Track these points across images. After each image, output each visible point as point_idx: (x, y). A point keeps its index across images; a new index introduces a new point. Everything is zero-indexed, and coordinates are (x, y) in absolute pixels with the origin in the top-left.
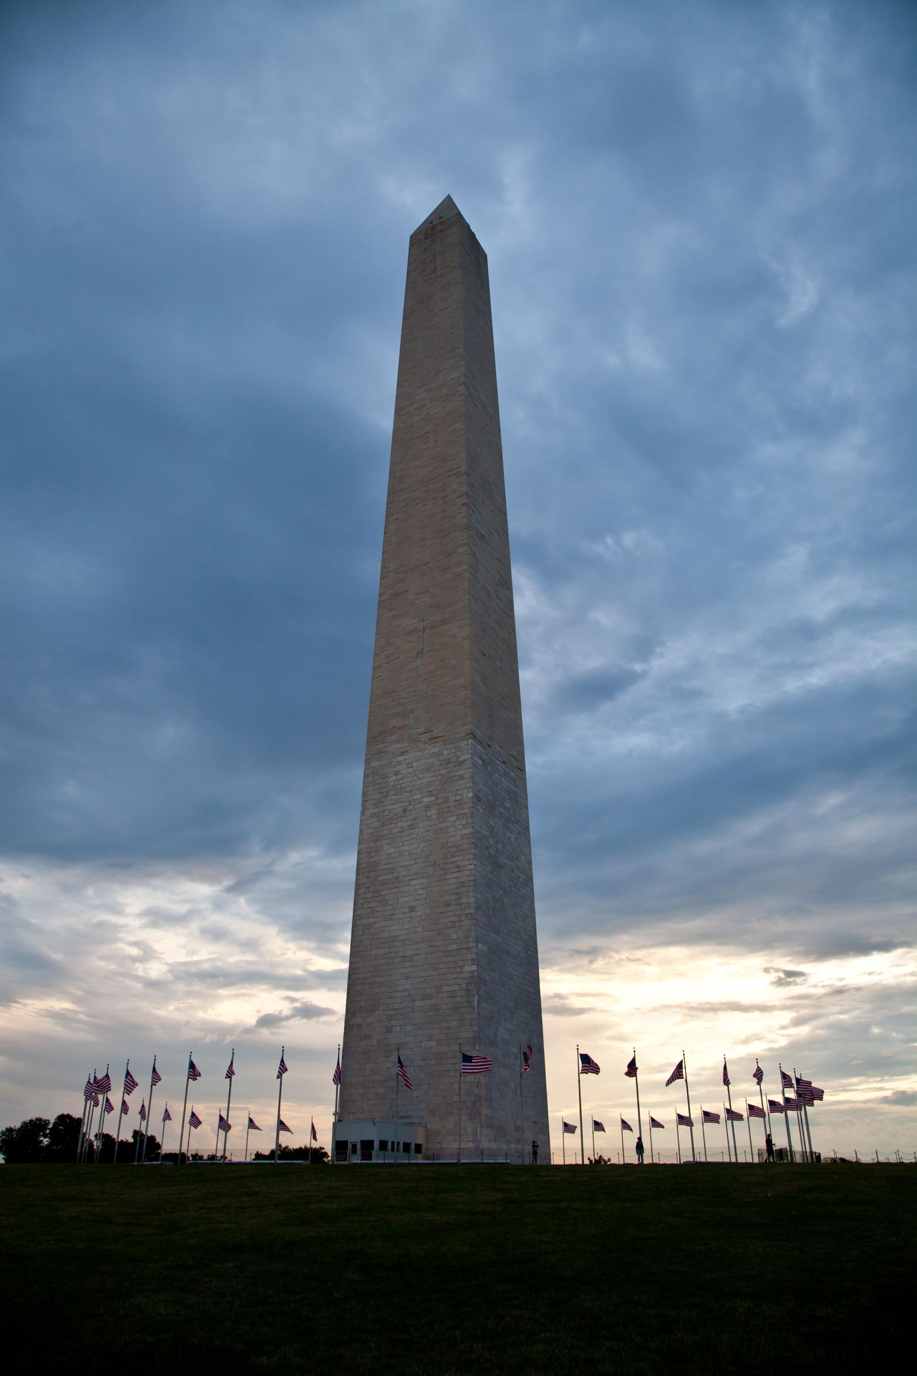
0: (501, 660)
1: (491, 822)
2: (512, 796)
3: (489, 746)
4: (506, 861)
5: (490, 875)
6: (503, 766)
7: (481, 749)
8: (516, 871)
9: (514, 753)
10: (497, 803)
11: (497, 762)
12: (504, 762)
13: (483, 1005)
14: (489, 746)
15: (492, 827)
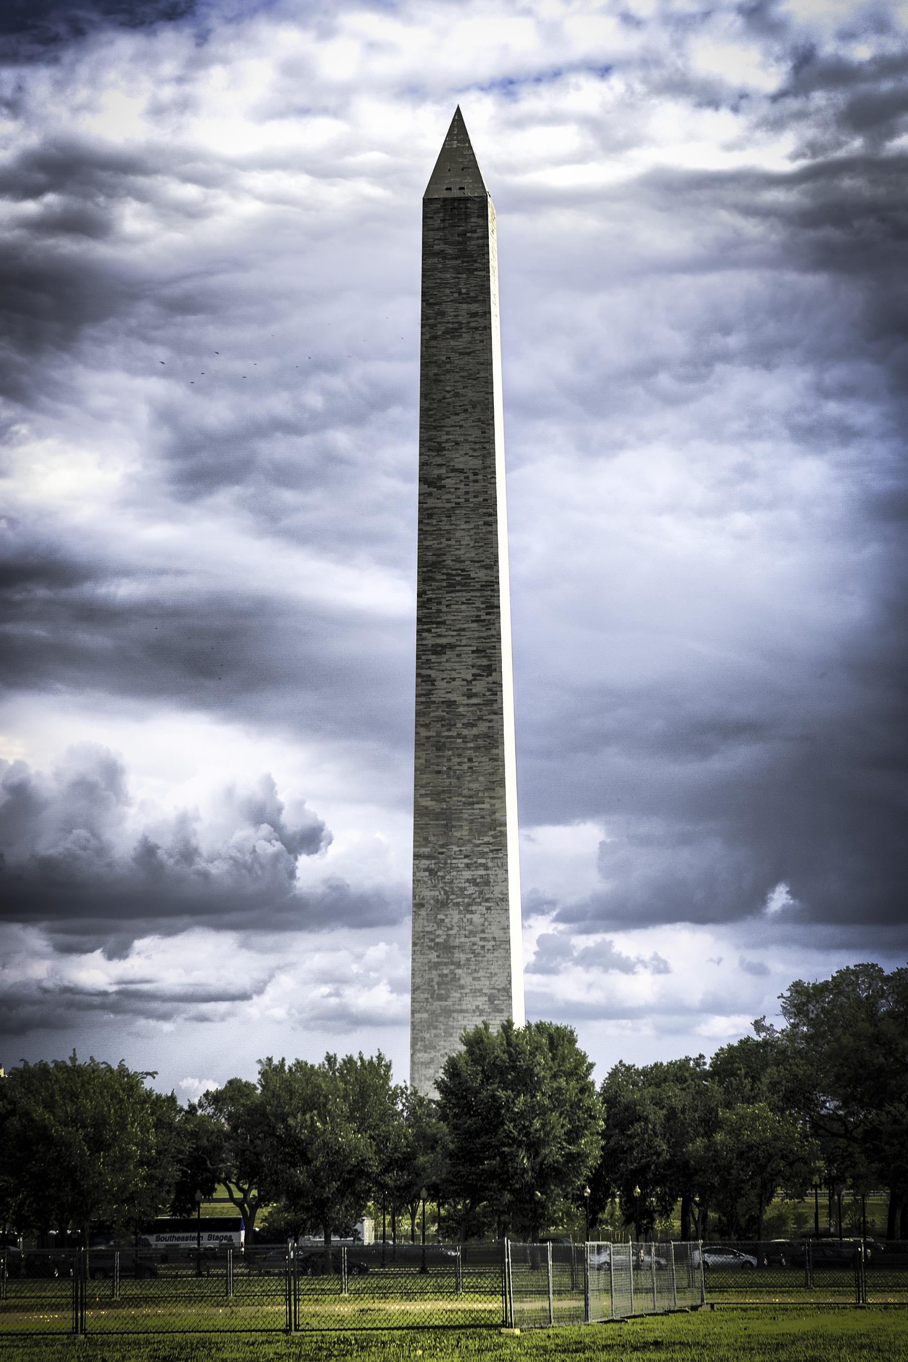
0: (470, 760)
1: (443, 917)
2: (478, 880)
3: (442, 853)
4: (463, 940)
5: (436, 960)
6: (466, 861)
7: (427, 862)
8: (482, 943)
9: (486, 839)
10: (451, 897)
11: (454, 861)
12: (466, 857)
13: (419, 1055)
14: (442, 853)
15: (442, 921)
